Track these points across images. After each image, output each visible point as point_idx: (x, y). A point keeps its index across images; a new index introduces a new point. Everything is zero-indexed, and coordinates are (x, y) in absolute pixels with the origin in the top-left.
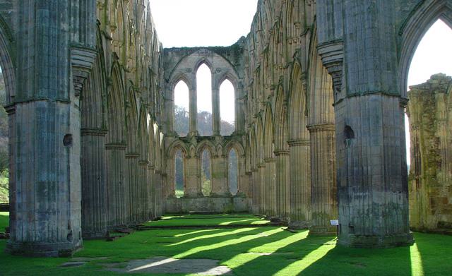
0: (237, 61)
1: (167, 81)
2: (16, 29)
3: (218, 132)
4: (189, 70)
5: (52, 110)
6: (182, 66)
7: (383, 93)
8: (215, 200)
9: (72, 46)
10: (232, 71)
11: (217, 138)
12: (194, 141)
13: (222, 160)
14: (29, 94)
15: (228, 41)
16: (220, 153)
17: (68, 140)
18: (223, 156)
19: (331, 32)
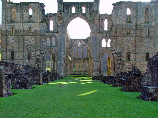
0: (87, 42)
1: (72, 46)
2: (57, 53)
3: (82, 57)
4: (77, 44)
5: (61, 62)
6: (75, 43)
7: (97, 61)
8: (81, 72)
9: (63, 55)
10: (86, 44)
11: (82, 59)
12: (77, 59)
13: (83, 64)
14: (59, 60)
15: (85, 37)
16: (83, 62)
17: (63, 65)
18: (84, 63)
19: (92, 54)
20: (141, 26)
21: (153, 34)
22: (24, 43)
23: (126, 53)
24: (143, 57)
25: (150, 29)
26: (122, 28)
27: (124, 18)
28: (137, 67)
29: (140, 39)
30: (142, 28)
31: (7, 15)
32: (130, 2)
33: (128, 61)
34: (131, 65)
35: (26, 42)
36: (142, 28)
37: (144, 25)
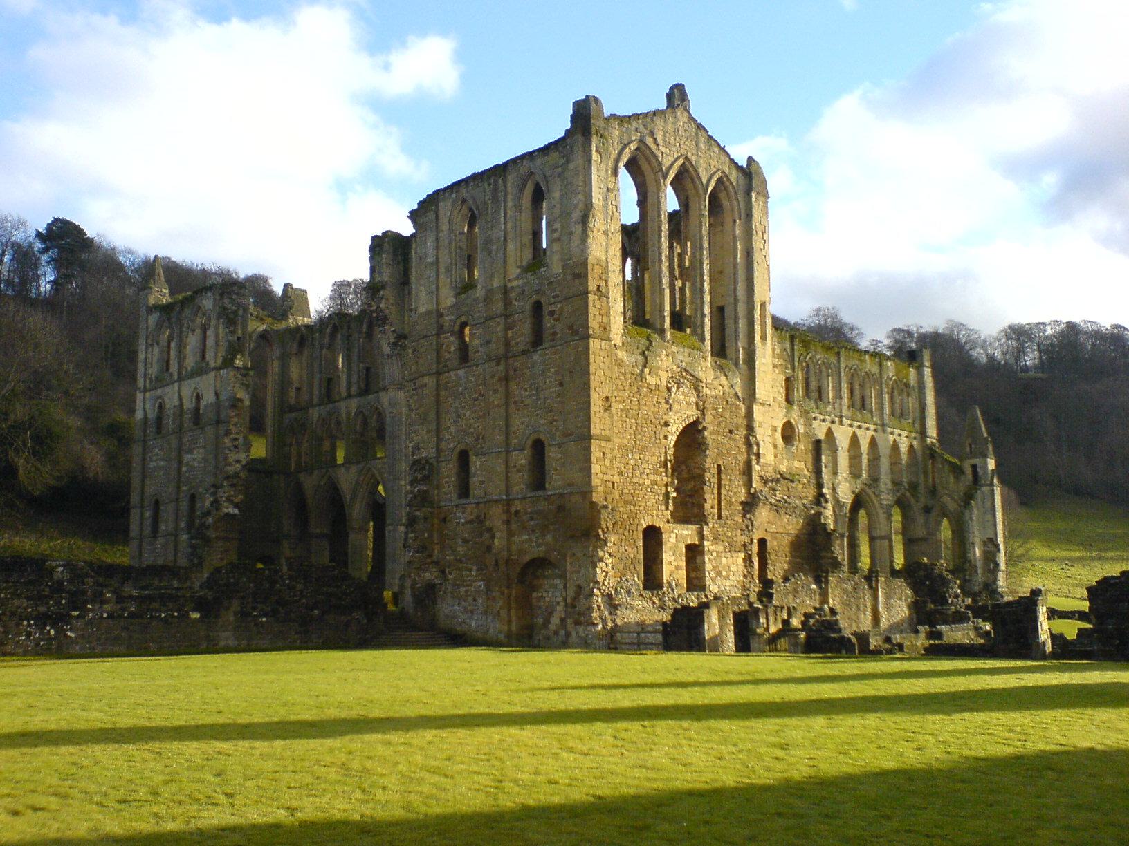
20: (505, 291)
21: (559, 326)
22: (180, 462)
23: (455, 457)
24: (519, 471)
25: (543, 301)
26: (442, 326)
27: (447, 270)
28: (490, 530)
29: (500, 368)
30: (507, 303)
31: (149, 360)
32: (514, 161)
33: (463, 501)
34: (471, 522)
35: (187, 457)
36: (507, 303)
37: (521, 282)
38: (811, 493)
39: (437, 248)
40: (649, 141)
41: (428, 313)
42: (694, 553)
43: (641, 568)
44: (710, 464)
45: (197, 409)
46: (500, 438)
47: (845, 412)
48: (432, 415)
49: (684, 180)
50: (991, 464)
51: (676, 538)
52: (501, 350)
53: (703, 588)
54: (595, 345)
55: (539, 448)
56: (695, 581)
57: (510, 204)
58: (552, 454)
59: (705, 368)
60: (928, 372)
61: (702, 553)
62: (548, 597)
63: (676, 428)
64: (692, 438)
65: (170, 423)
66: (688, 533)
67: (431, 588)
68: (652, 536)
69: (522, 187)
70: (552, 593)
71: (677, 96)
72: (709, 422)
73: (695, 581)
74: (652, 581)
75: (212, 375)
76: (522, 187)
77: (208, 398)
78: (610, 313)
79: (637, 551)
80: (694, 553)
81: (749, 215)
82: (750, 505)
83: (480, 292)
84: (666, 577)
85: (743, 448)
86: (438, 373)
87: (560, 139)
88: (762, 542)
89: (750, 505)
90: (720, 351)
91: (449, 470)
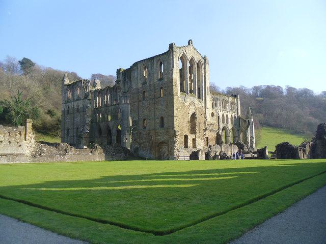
28: (151, 136)
36: (154, 87)
38: (217, 127)
39: (137, 74)
40: (185, 53)
41: (136, 88)
42: (194, 140)
43: (184, 143)
44: (197, 122)
45: (78, 108)
46: (153, 116)
47: (221, 109)
48: (137, 111)
49: (192, 61)
50: (252, 120)
51: (191, 137)
52: (153, 97)
53: (196, 148)
54: (175, 97)
55: (162, 119)
56: (194, 146)
57: (155, 66)
58: (165, 120)
59: (196, 100)
60: (239, 100)
61: (196, 140)
62: (164, 150)
63: (191, 114)
64: (194, 116)
65: (71, 111)
66: (193, 136)
67: (137, 148)
68: (186, 137)
69: (157, 62)
70: (164, 149)
71: (190, 42)
72: (197, 113)
73: (194, 146)
74: (186, 146)
75: (82, 101)
76: (157, 62)
77: (81, 106)
78: (177, 89)
79: (183, 140)
80: (194, 140)
81: (205, 68)
82: (205, 130)
83: (148, 84)
84: (189, 145)
85: (204, 118)
86: (139, 102)
87: (165, 53)
88: (207, 138)
89: (205, 130)
90: (199, 97)
91: (141, 123)
